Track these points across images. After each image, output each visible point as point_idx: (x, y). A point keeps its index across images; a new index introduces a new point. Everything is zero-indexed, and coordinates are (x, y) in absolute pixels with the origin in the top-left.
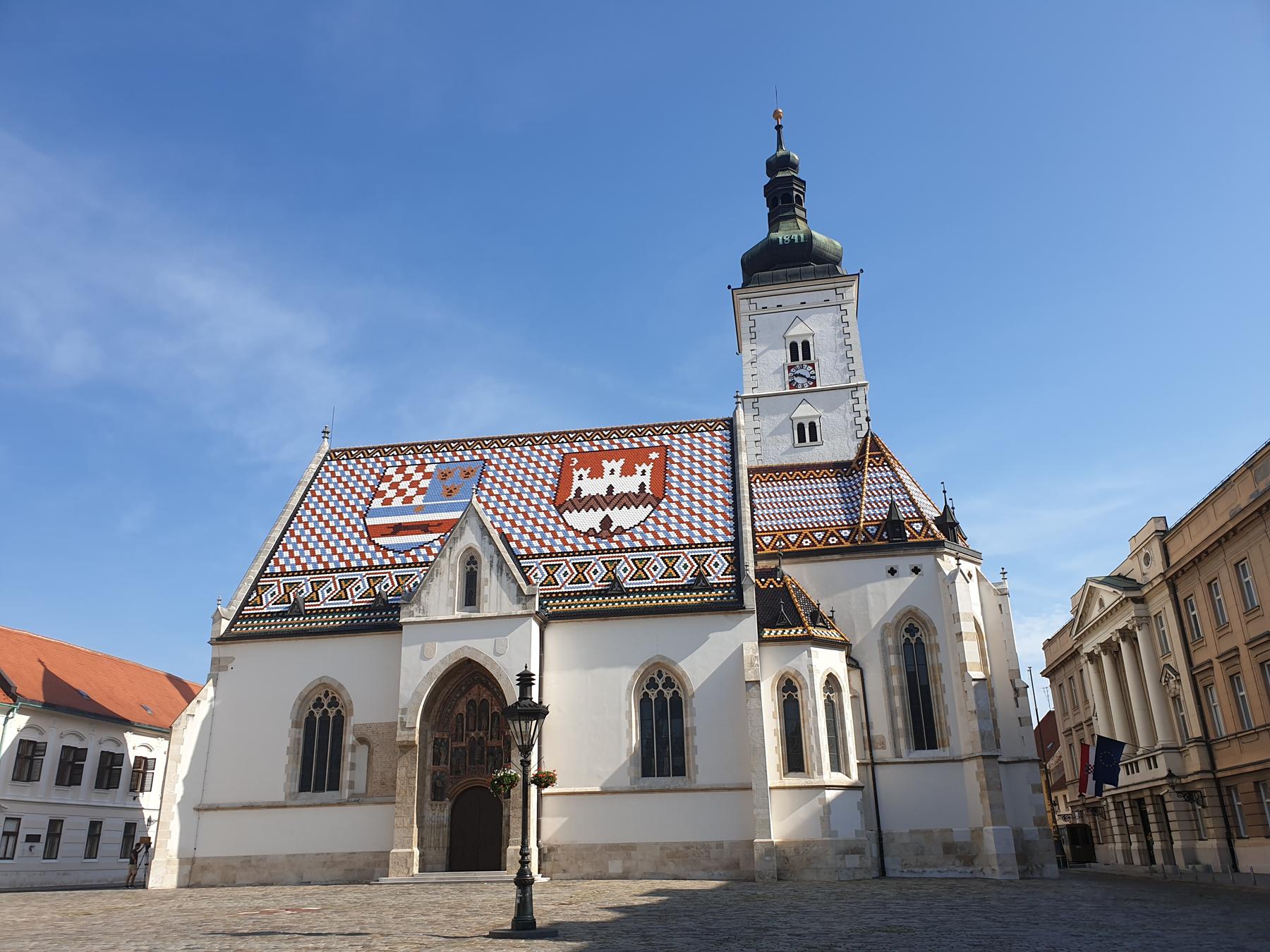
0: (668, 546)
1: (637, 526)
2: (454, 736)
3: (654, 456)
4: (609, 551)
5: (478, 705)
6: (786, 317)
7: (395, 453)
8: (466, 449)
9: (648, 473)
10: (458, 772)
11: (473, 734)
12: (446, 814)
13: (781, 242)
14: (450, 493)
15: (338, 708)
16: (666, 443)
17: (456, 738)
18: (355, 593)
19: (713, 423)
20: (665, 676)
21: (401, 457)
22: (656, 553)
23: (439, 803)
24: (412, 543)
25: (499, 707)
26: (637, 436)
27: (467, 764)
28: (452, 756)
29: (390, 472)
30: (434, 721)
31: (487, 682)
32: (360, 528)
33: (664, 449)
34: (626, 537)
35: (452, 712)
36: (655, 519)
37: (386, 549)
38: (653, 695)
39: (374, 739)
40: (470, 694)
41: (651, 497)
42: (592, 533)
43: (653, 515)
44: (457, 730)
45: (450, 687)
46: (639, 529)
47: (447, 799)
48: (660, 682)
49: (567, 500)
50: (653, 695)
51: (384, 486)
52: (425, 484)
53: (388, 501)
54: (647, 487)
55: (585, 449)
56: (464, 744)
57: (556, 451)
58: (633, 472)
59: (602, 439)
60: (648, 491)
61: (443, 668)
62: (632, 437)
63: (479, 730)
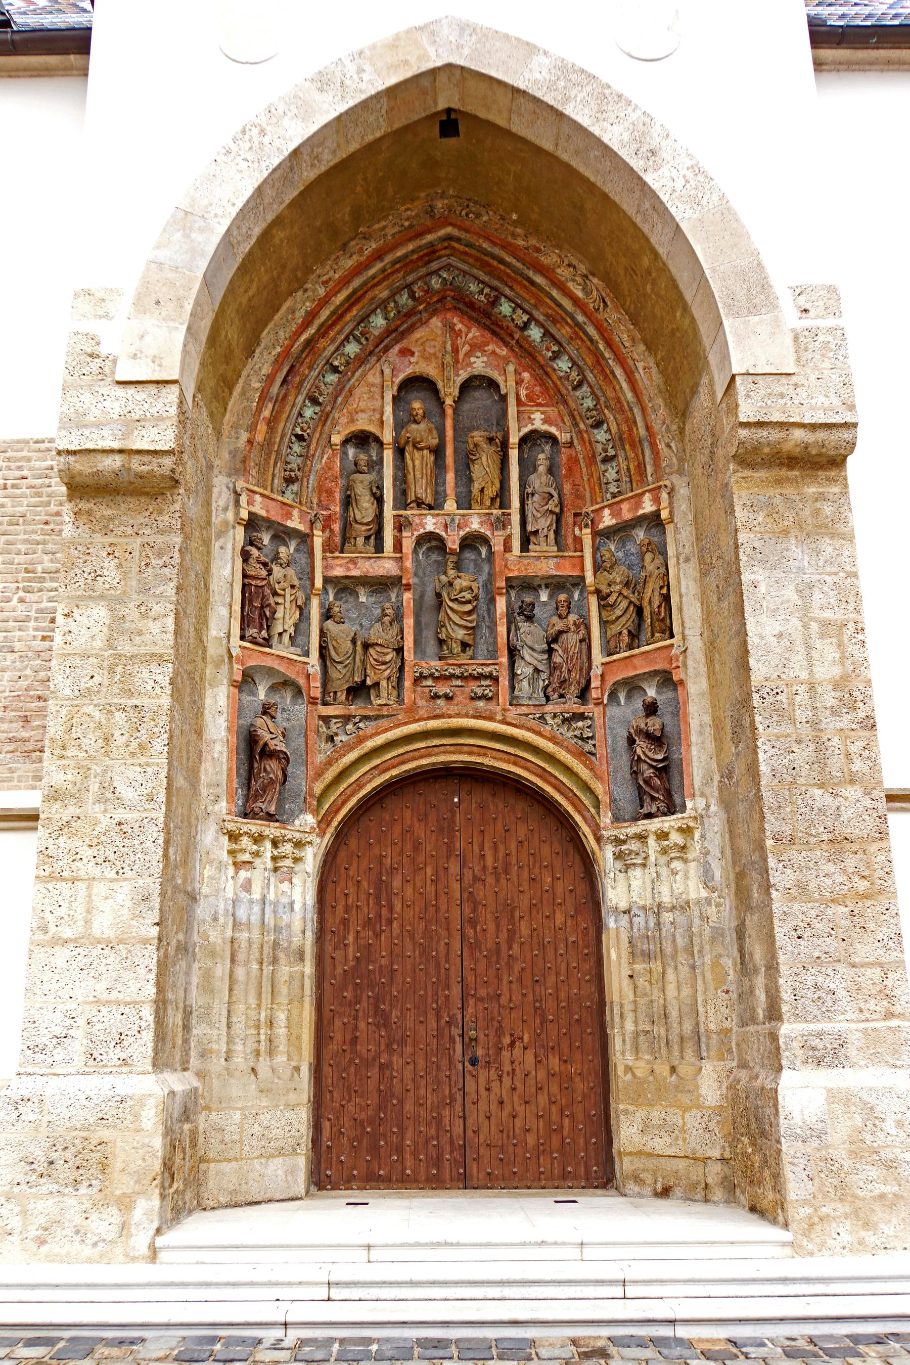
2: (337, 527)
5: (450, 393)
10: (359, 691)
17: (345, 539)
23: (272, 830)
25: (552, 411)
27: (409, 655)
28: (327, 615)
30: (244, 436)
31: (495, 302)
35: (324, 418)
40: (406, 352)
44: (348, 502)
45: (322, 292)
47: (309, 819)
56: (386, 567)
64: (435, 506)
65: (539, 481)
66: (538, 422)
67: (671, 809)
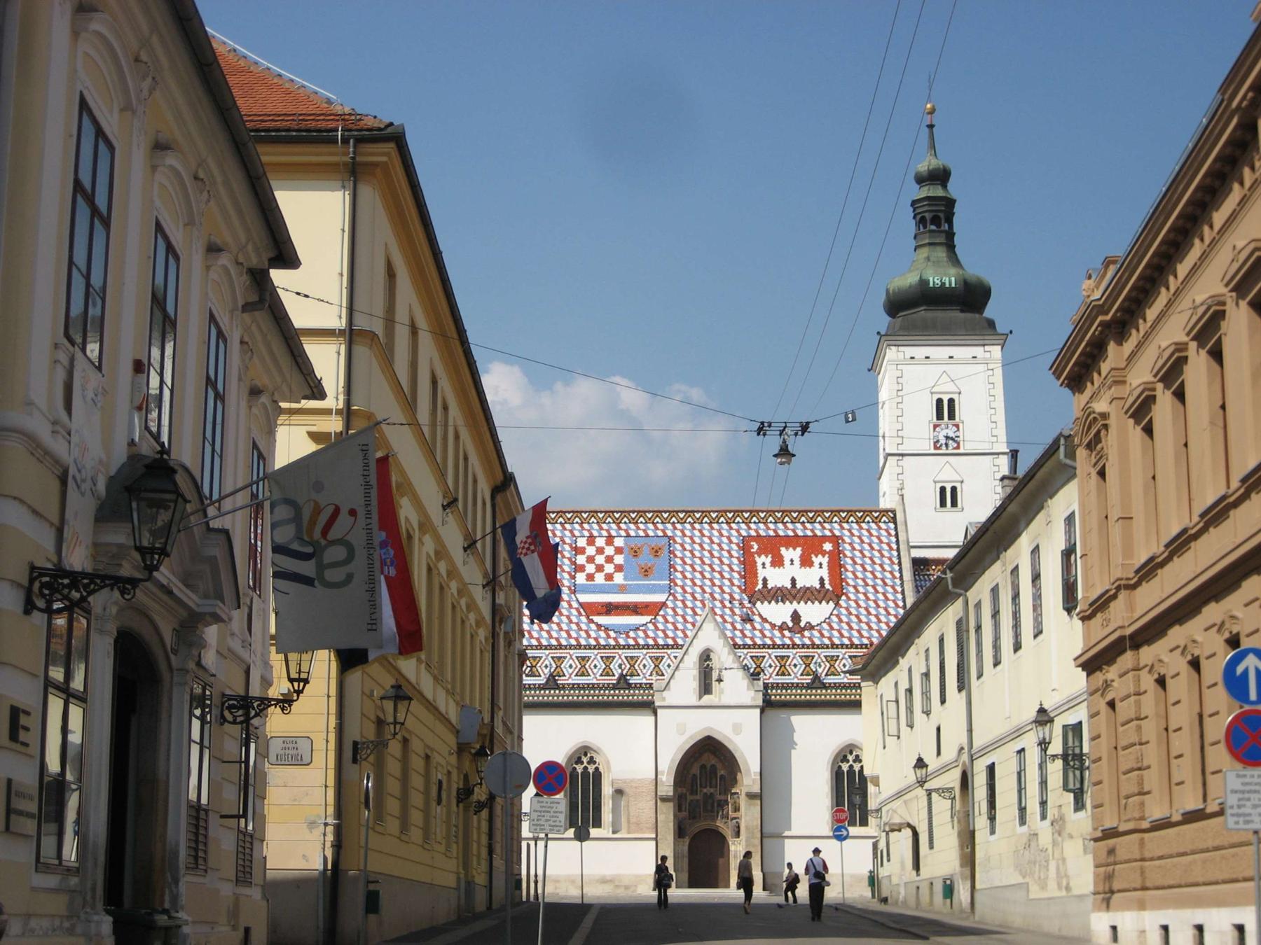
0: (852, 645)
1: (825, 622)
3: (828, 546)
4: (803, 646)
5: (708, 766)
6: (933, 372)
7: (579, 521)
8: (646, 522)
9: (825, 565)
10: (694, 818)
11: (705, 790)
12: (686, 848)
13: (931, 285)
14: (646, 572)
15: (596, 765)
16: (837, 533)
18: (595, 671)
19: (878, 514)
20: (854, 753)
21: (586, 526)
22: (844, 651)
23: (682, 840)
24: (629, 625)
26: (808, 522)
29: (582, 542)
32: (575, 605)
33: (835, 540)
34: (816, 633)
36: (837, 616)
37: (607, 629)
38: (845, 767)
39: (627, 790)
41: (833, 592)
42: (785, 627)
43: (835, 612)
46: (825, 625)
48: (851, 758)
49: (757, 589)
50: (845, 767)
51: (581, 560)
52: (619, 559)
53: (590, 577)
54: (827, 582)
55: (762, 533)
56: (698, 797)
57: (734, 533)
58: (811, 564)
59: (776, 522)
60: (827, 586)
61: (692, 742)
62: (803, 522)
63: (711, 787)
64: (706, 787)
65: (723, 782)
66: (722, 772)
67: (739, 837)
